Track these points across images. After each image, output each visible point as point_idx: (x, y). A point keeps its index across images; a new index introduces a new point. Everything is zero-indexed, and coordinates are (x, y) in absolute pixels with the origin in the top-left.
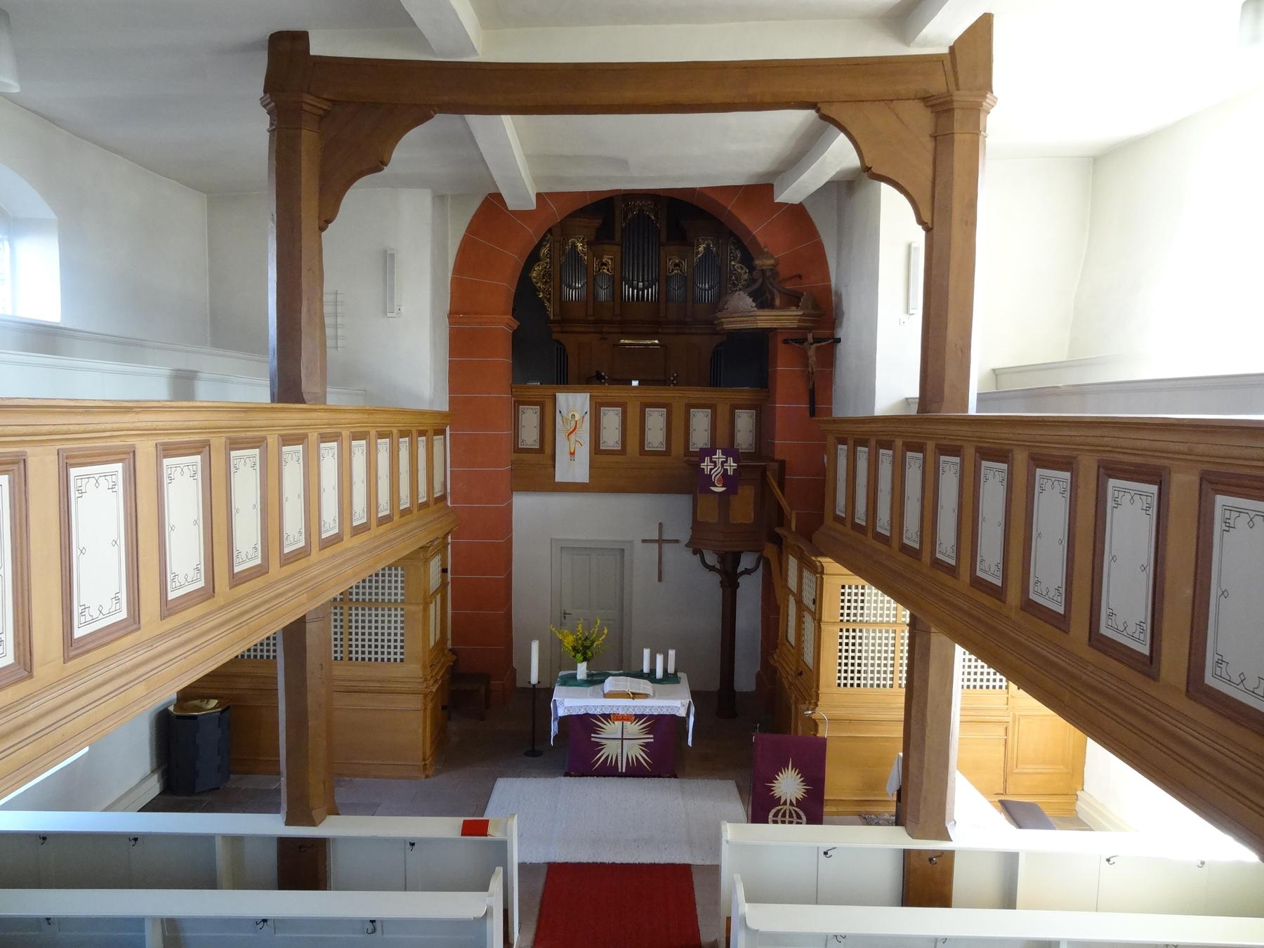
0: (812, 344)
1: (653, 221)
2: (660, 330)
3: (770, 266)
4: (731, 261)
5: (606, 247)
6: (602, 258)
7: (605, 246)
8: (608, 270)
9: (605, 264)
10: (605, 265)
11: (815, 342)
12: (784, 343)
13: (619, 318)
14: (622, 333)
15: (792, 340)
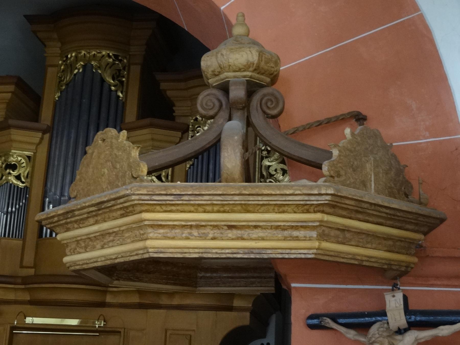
0: (400, 332)
1: (110, 86)
2: (109, 299)
3: (246, 68)
4: (262, 158)
5: (16, 135)
6: (7, 155)
7: (13, 131)
8: (18, 177)
9: (14, 167)
10: (14, 167)
11: (412, 325)
12: (312, 327)
13: (31, 272)
14: (32, 303)
15: (334, 318)
